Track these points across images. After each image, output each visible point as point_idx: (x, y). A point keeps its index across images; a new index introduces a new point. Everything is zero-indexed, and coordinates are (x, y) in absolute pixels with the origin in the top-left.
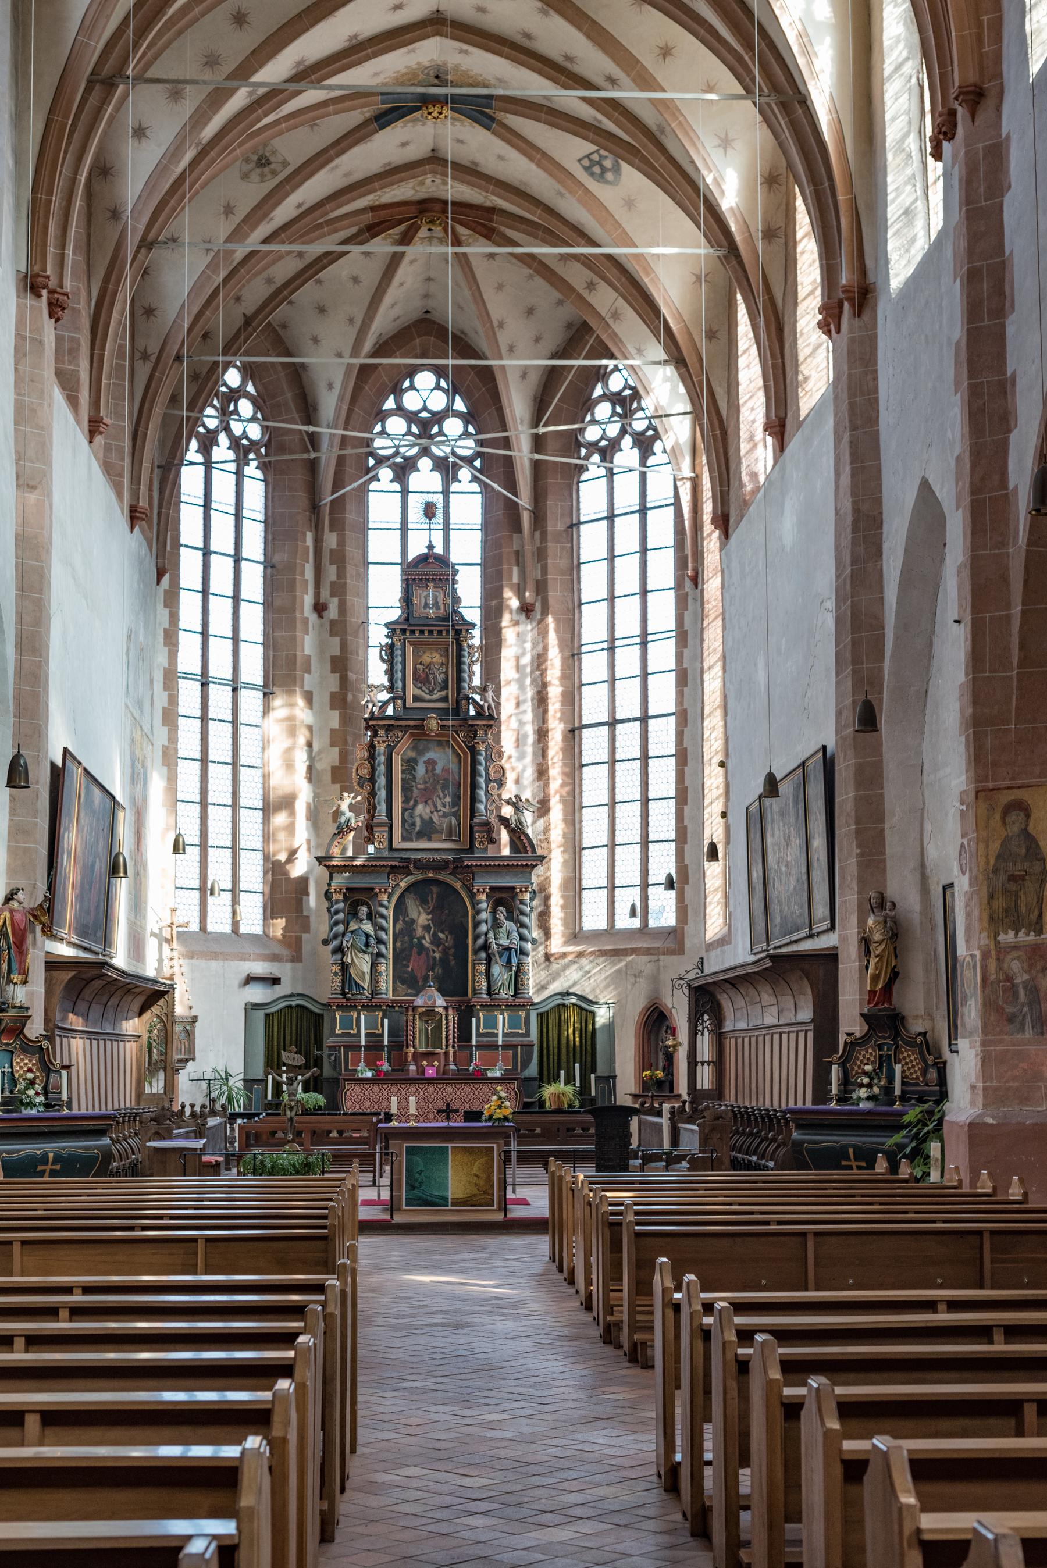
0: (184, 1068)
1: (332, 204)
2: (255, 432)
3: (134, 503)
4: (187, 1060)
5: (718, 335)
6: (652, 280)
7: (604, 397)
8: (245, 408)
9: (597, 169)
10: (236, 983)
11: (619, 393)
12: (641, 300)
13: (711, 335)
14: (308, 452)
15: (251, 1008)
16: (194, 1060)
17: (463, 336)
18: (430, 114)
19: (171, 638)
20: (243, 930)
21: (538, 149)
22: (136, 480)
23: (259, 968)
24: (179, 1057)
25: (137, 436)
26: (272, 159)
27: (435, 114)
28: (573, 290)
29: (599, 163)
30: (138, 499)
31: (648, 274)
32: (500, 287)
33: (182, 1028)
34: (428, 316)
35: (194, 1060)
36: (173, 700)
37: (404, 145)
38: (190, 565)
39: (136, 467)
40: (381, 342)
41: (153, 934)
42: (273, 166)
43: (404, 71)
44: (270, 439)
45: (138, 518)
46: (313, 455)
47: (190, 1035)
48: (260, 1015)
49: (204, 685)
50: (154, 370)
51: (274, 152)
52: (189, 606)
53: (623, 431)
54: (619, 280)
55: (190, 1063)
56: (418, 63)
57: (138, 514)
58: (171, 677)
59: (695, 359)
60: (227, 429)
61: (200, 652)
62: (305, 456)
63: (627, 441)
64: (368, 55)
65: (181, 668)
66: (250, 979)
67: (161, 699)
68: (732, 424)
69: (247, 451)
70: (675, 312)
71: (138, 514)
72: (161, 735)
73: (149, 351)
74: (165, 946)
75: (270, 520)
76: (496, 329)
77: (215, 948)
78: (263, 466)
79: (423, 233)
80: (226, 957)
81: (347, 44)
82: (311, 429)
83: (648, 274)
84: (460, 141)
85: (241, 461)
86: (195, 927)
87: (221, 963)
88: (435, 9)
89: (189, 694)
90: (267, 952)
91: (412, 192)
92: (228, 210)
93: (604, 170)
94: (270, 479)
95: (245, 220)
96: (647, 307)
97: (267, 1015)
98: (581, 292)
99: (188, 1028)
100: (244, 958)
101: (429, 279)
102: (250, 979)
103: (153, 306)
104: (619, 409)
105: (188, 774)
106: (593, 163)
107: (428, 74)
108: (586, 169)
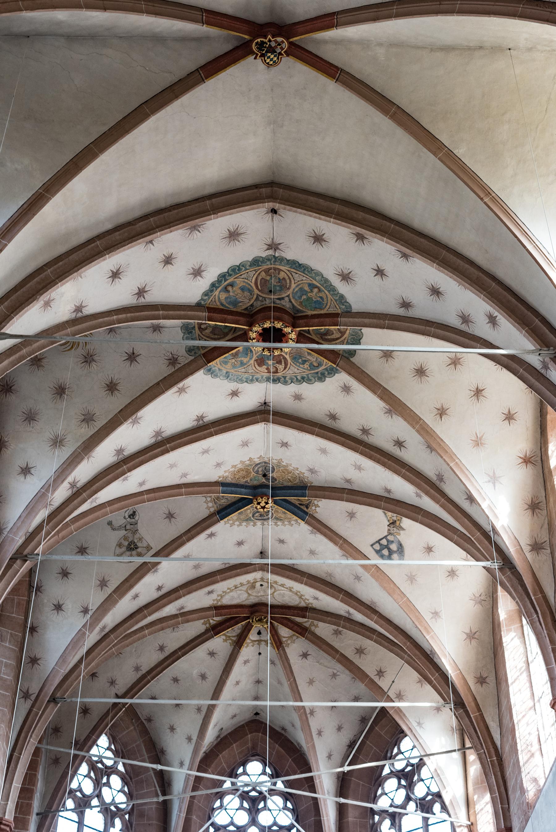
1: (185, 590)
5: (488, 680)
6: (432, 637)
7: (393, 774)
9: (385, 552)
11: (403, 770)
12: (423, 658)
13: (481, 680)
14: (157, 796)
17: (283, 732)
18: (259, 503)
21: (341, 537)
26: (139, 544)
27: (263, 504)
28: (367, 676)
29: (387, 547)
30: (5, 816)
31: (428, 633)
32: (311, 682)
34: (257, 718)
37: (240, 543)
40: (222, 736)
42: (139, 550)
43: (240, 466)
46: (161, 799)
50: (33, 706)
51: (141, 539)
53: (408, 799)
54: (405, 644)
56: (250, 459)
59: (471, 699)
62: (155, 800)
63: (412, 806)
64: (211, 433)
68: (507, 748)
70: (452, 662)
76: (309, 716)
79: (253, 636)
81: (195, 423)
82: (159, 767)
83: (428, 633)
84: (282, 541)
88: (262, 401)
91: (246, 595)
92: (103, 584)
93: (391, 552)
95: (115, 591)
96: (426, 663)
98: (373, 677)
101: (258, 682)
103: (38, 656)
104: (403, 782)
106: (383, 547)
107: (257, 472)
108: (378, 552)
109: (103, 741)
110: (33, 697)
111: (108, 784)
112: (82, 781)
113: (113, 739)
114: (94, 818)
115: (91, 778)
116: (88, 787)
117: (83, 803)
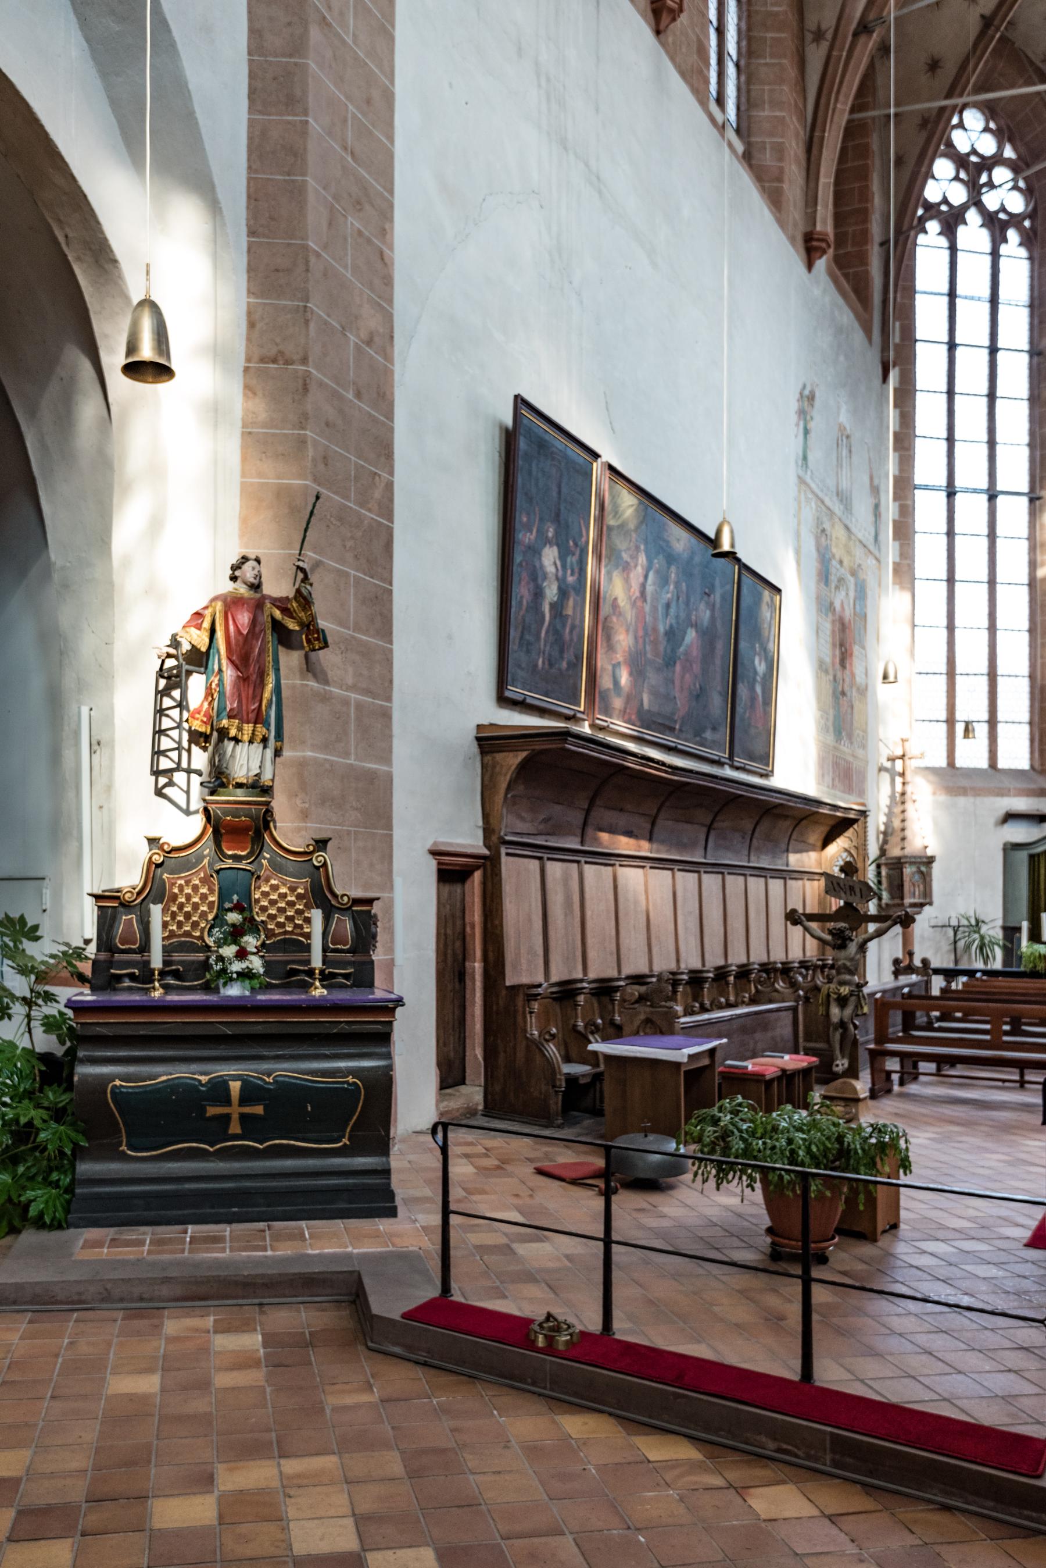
0: (919, 913)
2: (1016, 204)
3: (809, 229)
4: (922, 905)
8: (1002, 174)
10: (992, 821)
15: (1011, 848)
16: (931, 904)
19: (905, 441)
20: (1001, 764)
22: (811, 200)
23: (1021, 804)
24: (912, 901)
25: (812, 147)
30: (815, 224)
33: (914, 869)
35: (931, 904)
36: (906, 512)
38: (929, 365)
39: (812, 185)
41: (881, 769)
44: (1035, 209)
45: (817, 249)
47: (926, 878)
48: (1023, 856)
49: (951, 494)
52: (929, 413)
55: (927, 908)
57: (815, 243)
58: (905, 486)
60: (979, 204)
61: (945, 460)
65: (918, 479)
66: (1010, 817)
67: (890, 510)
69: (1004, 226)
71: (815, 243)
72: (891, 551)
73: (824, 27)
74: (899, 780)
75: (1036, 303)
77: (964, 783)
78: (1028, 240)
80: (977, 792)
85: (998, 238)
86: (943, 763)
87: (971, 799)
89: (928, 509)
90: (1033, 786)
94: (1036, 255)
97: (1032, 857)
99: (923, 869)
100: (1001, 793)
102: (1010, 817)
105: (931, 595)
109: (973, 119)
110: (829, 35)
111: (991, 185)
112: (943, 184)
113: (990, 110)
114: (973, 234)
115: (961, 180)
116: (958, 195)
117: (951, 221)
